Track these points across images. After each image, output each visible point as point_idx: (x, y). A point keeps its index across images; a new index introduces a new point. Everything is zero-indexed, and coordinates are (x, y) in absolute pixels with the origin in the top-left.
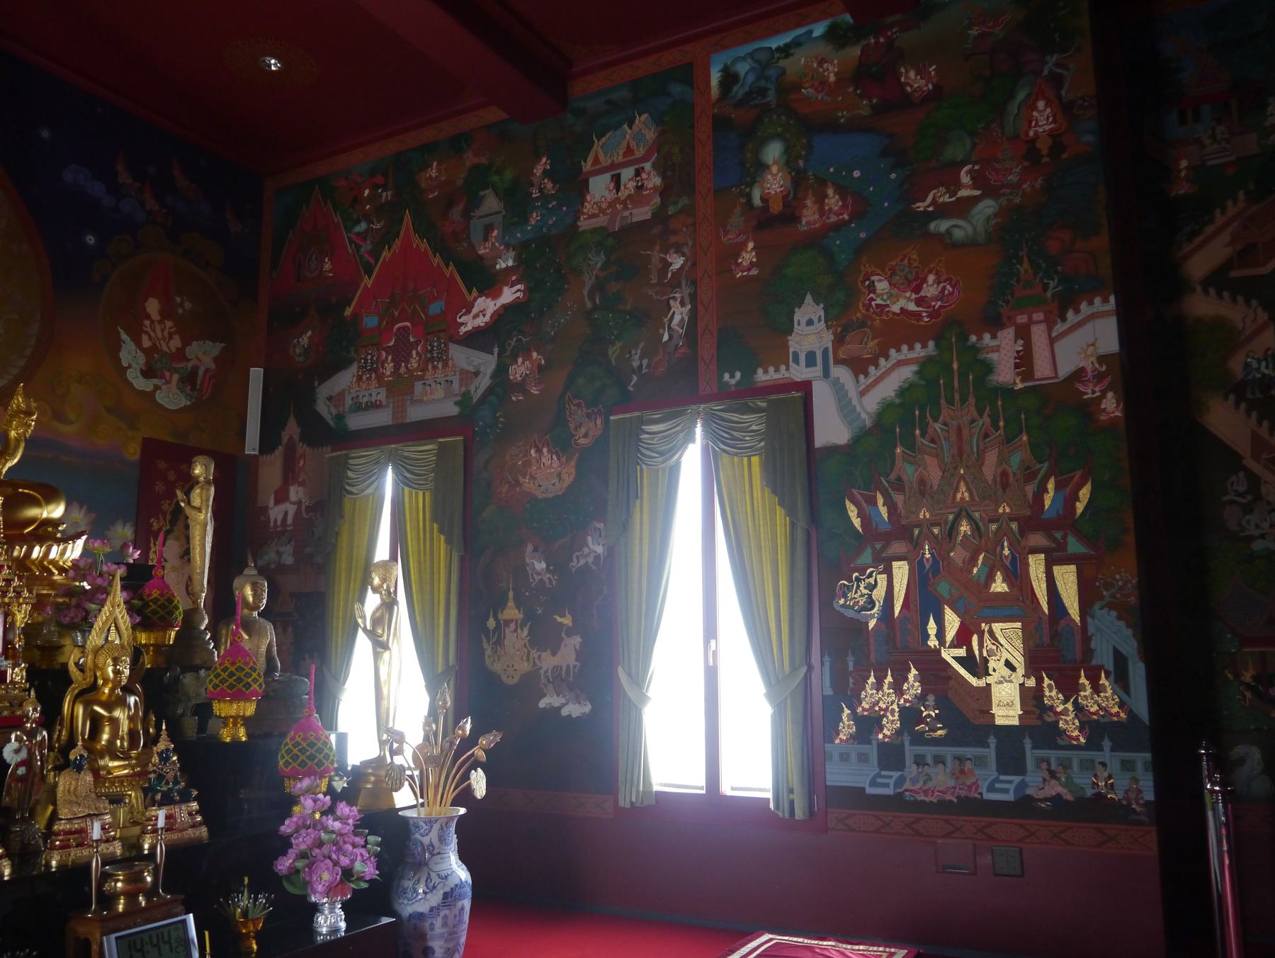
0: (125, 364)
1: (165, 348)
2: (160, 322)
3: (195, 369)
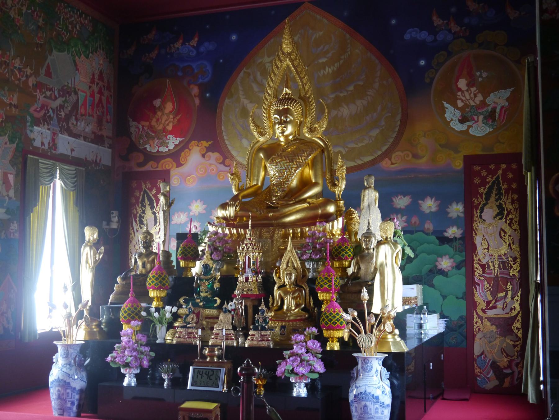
0: (448, 120)
1: (472, 103)
2: (467, 91)
3: (494, 110)
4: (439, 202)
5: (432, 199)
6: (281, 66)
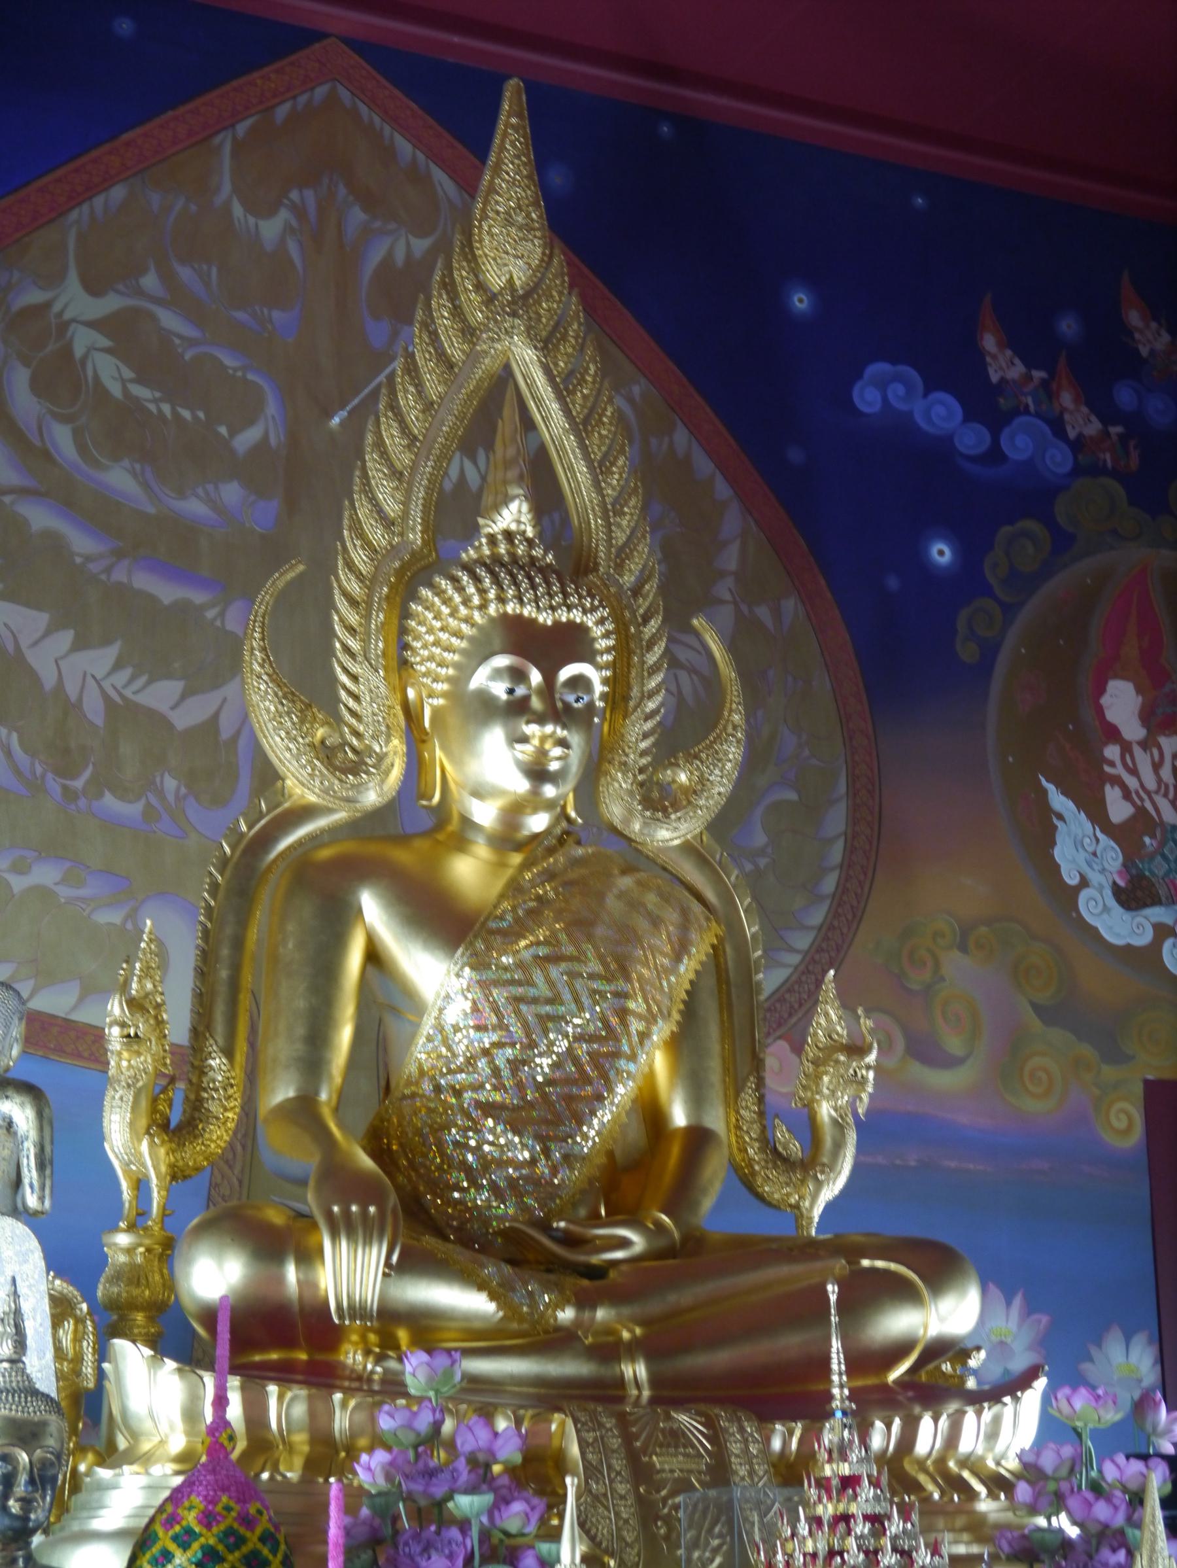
0: (1072, 880)
2: (1145, 745)
4: (1045, 1319)
5: (1009, 1303)
6: (473, 357)
